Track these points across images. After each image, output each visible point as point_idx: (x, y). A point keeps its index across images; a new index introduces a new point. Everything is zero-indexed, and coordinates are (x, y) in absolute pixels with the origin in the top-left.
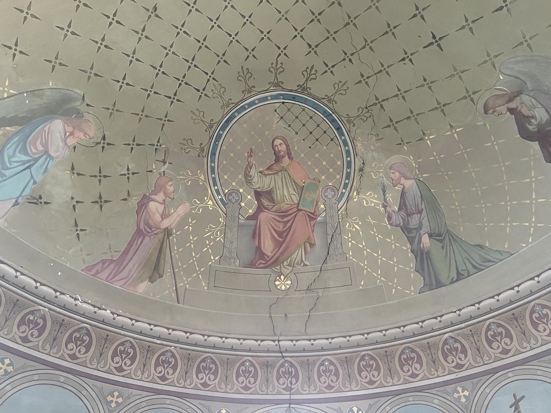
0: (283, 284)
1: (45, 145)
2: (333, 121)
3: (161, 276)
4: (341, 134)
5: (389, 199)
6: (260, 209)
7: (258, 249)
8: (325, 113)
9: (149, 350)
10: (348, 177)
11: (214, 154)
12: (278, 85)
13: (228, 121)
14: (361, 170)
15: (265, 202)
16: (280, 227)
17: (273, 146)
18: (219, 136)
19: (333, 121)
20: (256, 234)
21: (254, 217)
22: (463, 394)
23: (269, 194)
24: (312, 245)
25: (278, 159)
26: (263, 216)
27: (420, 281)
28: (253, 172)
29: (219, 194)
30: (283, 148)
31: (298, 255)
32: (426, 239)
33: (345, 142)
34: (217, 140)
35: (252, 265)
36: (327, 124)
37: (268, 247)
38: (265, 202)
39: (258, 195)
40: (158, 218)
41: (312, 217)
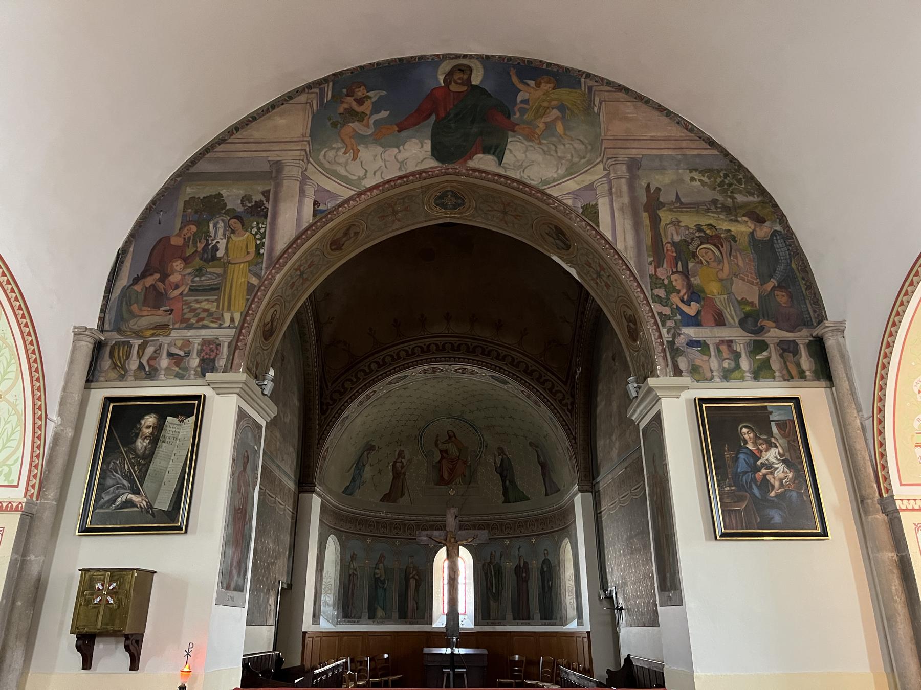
0: (452, 492)
1: (363, 463)
2: (474, 428)
3: (404, 495)
4: (477, 432)
5: (497, 460)
6: (442, 458)
7: (442, 476)
8: (470, 425)
9: (405, 525)
10: (480, 448)
11: (421, 437)
12: (450, 415)
13: (427, 426)
14: (486, 446)
15: (444, 455)
16: (451, 466)
17: (448, 434)
18: (423, 431)
19: (474, 428)
20: (440, 470)
21: (440, 462)
22: (507, 542)
23: (446, 451)
24: (465, 476)
25: (450, 437)
26: (443, 462)
27: (502, 498)
28: (439, 442)
29: (423, 452)
30: (452, 434)
31: (459, 480)
32: (507, 482)
33: (479, 435)
34: (422, 433)
35: (438, 484)
36: (471, 428)
37: (446, 476)
38: (444, 455)
39: (441, 451)
40: (400, 469)
41: (465, 462)
